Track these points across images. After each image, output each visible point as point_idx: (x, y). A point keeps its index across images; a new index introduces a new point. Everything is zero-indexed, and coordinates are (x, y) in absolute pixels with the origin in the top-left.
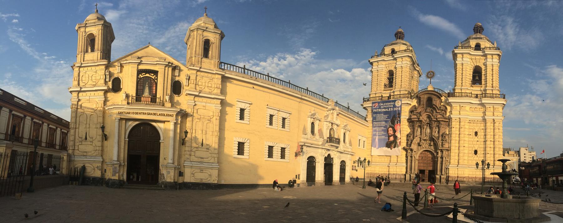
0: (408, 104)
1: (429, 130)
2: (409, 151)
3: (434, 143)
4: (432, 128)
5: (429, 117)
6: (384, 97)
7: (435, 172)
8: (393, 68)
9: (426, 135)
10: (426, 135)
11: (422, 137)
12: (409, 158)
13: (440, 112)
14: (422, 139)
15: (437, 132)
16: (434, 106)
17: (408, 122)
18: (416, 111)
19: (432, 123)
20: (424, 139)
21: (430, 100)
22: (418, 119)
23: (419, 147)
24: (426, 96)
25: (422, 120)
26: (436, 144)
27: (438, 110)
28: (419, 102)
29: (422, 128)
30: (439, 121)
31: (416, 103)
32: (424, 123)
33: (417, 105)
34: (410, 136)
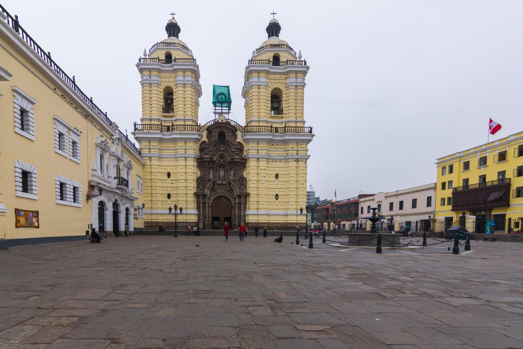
0: (197, 138)
1: (223, 172)
2: (201, 197)
3: (230, 188)
4: (227, 170)
5: (222, 157)
6: (163, 126)
7: (233, 219)
8: (171, 85)
9: (219, 178)
10: (219, 178)
11: (216, 181)
12: (201, 205)
13: (236, 151)
14: (216, 184)
15: (232, 175)
16: (229, 143)
17: (197, 162)
18: (208, 148)
19: (226, 164)
20: (218, 183)
21: (222, 135)
22: (211, 159)
23: (213, 193)
24: (218, 130)
25: (215, 161)
26: (234, 189)
27: (235, 149)
28: (209, 135)
29: (216, 170)
30: (235, 162)
31: (206, 138)
32: (217, 164)
33: (207, 141)
34: (201, 180)
